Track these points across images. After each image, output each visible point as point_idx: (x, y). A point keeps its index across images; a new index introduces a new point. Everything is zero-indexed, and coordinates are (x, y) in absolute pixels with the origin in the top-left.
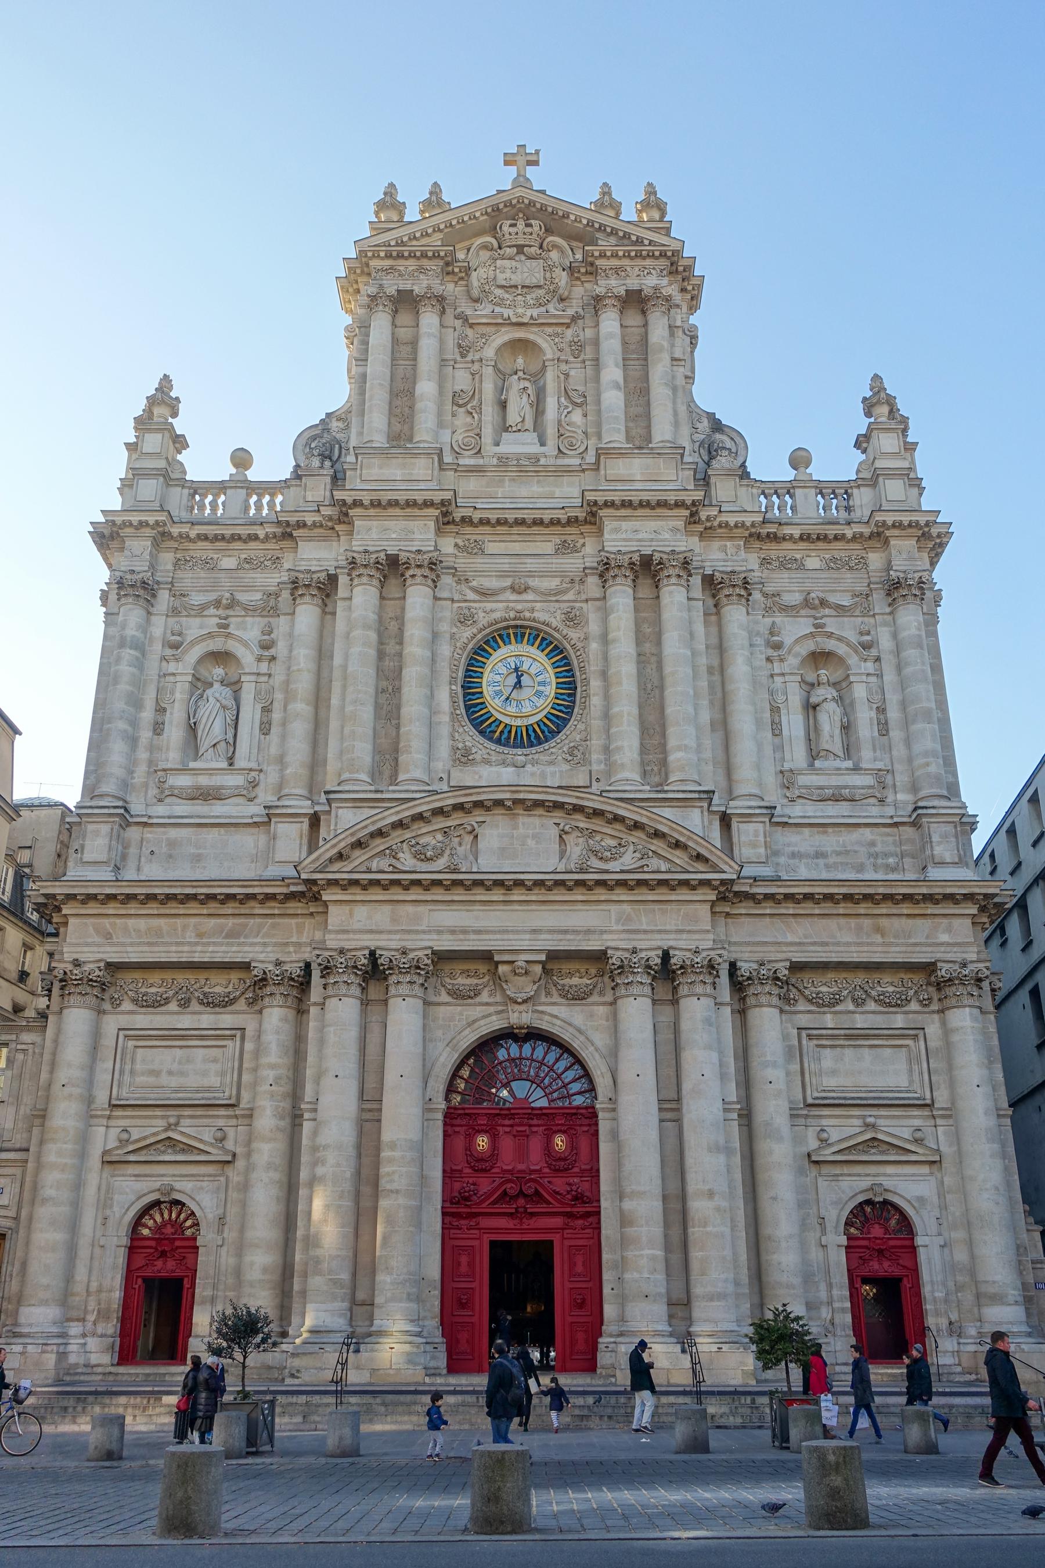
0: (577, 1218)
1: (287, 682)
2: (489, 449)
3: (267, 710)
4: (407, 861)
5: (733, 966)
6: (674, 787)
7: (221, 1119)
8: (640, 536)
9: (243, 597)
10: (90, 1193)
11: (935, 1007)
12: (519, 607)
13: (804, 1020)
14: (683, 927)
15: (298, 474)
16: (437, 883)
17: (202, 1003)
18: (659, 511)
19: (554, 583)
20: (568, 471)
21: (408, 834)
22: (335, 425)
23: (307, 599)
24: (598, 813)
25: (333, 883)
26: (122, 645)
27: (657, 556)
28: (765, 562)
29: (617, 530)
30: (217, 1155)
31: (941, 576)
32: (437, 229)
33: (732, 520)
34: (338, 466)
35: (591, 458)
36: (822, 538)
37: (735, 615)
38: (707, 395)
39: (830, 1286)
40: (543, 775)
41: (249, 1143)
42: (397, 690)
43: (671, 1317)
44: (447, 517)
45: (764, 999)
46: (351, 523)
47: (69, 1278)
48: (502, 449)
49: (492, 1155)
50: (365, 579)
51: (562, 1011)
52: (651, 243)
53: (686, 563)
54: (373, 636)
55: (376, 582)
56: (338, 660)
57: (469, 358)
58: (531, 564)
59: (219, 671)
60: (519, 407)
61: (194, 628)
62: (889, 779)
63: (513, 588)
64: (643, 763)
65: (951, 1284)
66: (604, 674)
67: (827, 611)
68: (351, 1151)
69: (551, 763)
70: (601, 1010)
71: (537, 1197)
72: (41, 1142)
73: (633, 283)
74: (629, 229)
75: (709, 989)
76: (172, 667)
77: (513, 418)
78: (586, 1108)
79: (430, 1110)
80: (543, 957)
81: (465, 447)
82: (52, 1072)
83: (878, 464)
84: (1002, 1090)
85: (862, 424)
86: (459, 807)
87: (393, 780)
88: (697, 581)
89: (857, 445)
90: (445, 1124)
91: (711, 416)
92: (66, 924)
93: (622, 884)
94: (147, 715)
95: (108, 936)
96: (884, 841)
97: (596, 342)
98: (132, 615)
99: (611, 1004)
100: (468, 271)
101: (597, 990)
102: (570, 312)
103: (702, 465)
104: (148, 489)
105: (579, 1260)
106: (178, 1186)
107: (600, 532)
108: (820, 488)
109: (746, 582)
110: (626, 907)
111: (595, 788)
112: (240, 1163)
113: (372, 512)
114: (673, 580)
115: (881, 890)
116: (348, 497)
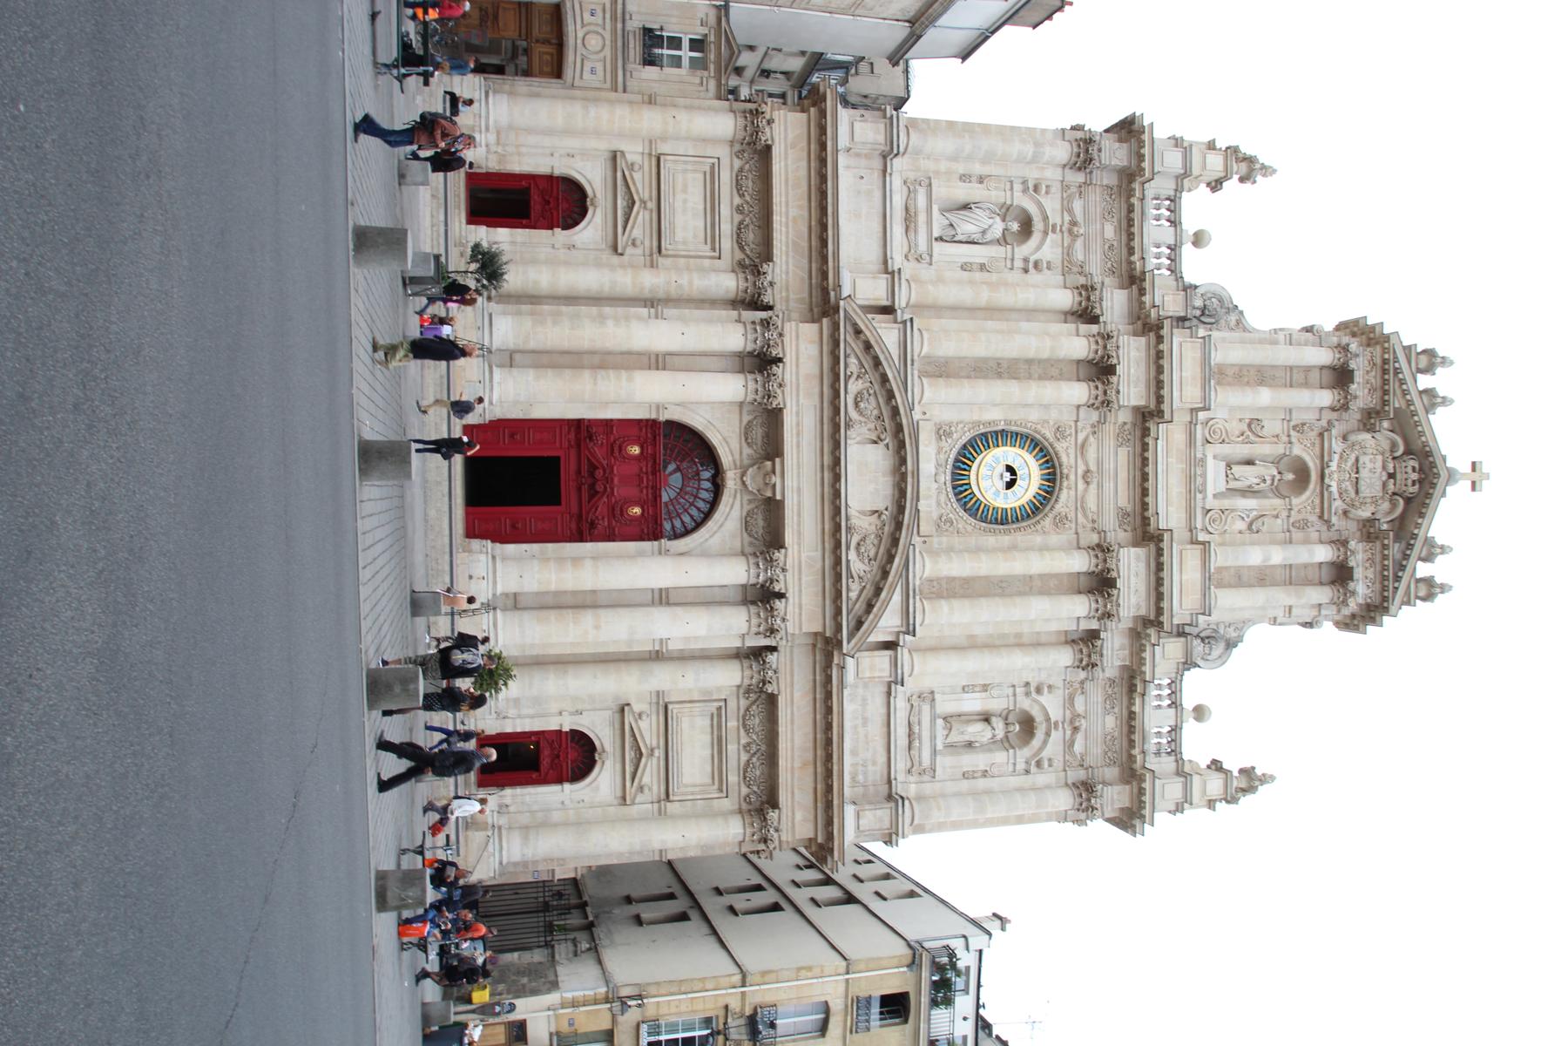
1: (1006, 284)
2: (1210, 451)
3: (982, 267)
4: (854, 387)
5: (773, 649)
6: (917, 604)
7: (649, 243)
8: (1133, 579)
9: (1079, 244)
10: (593, 143)
11: (745, 806)
12: (1072, 477)
13: (732, 704)
14: (802, 610)
15: (1189, 289)
16: (836, 411)
17: (741, 223)
18: (1153, 594)
19: (1091, 504)
21: (877, 387)
22: (1233, 318)
23: (1078, 299)
24: (895, 542)
25: (835, 327)
26: (1037, 144)
27: (1115, 592)
28: (1112, 682)
29: (1138, 558)
30: (621, 241)
31: (1099, 828)
32: (1410, 403)
33: (1147, 655)
34: (1195, 322)
35: (1202, 537)
36: (1131, 730)
37: (1066, 657)
38: (1258, 637)
39: (532, 717)
40: (928, 497)
41: (632, 266)
42: (999, 375)
43: (506, 595)
44: (1148, 417)
45: (748, 673)
46: (1143, 334)
47: (530, 131)
48: (1210, 462)
50: (1094, 347)
52: (1396, 588)
53: (1109, 615)
54: (1045, 355)
55: (1091, 356)
56: (1025, 325)
57: (1292, 433)
58: (1109, 486)
59: (1015, 226)
60: (1249, 476)
61: (1052, 204)
62: (926, 778)
63: (1088, 471)
64: (939, 579)
65: (535, 807)
66: (1014, 547)
67: (1069, 733)
68: (625, 348)
69: (939, 504)
70: (738, 545)
71: (593, 493)
72: (631, 103)
73: (1358, 573)
74: (1409, 569)
75: (754, 629)
76: (1018, 187)
77: (1237, 469)
80: (778, 497)
81: (1212, 432)
82: (685, 107)
83: (1196, 778)
84: (680, 855)
85: (1233, 765)
86: (899, 428)
87: (924, 374)
88: (1094, 625)
89: (1214, 762)
91: (1240, 639)
92: (803, 111)
93: (837, 562)
94: (978, 169)
95: (793, 146)
96: (876, 772)
97: (1306, 541)
98: (1063, 152)
100: (1371, 429)
102: (1334, 520)
103: (1194, 631)
104: (1172, 161)
106: (599, 212)
107: (1136, 544)
108: (1175, 730)
109: (1094, 665)
110: (819, 565)
111: (916, 540)
112: (615, 259)
113: (1153, 352)
114: (1094, 605)
115: (835, 768)
116: (1165, 332)
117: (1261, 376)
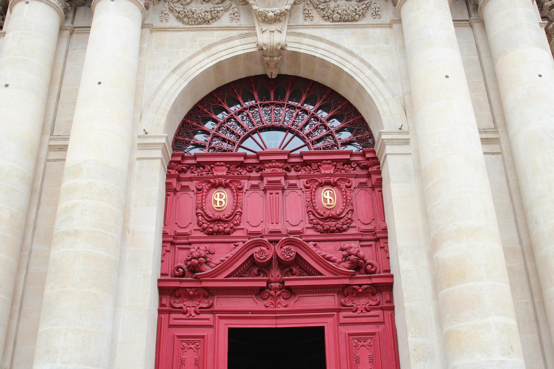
0: (359, 295)
49: (234, 214)
51: (329, 33)
78: (363, 155)
79: (144, 146)
90: (169, 176)
99: (390, 26)
101: (370, 11)
105: (364, 354)
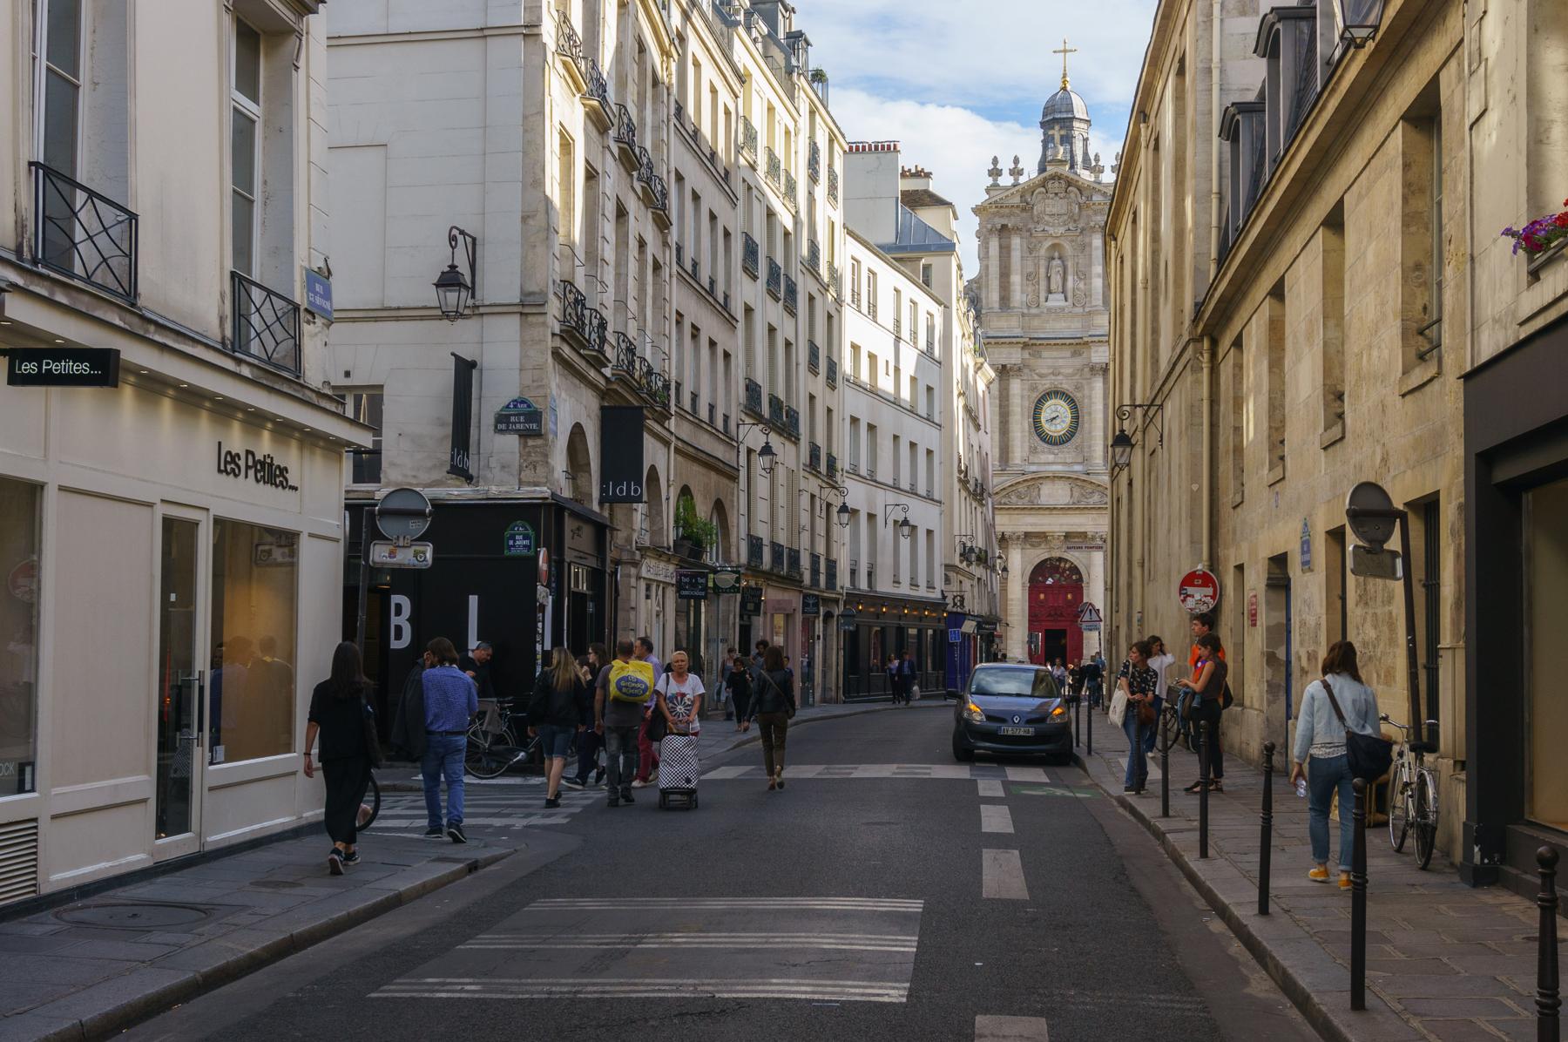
20: (1077, 315)
48: (1049, 304)
58: (1061, 362)
77: (1053, 287)
97: (1090, 244)
117: (1005, 274)
